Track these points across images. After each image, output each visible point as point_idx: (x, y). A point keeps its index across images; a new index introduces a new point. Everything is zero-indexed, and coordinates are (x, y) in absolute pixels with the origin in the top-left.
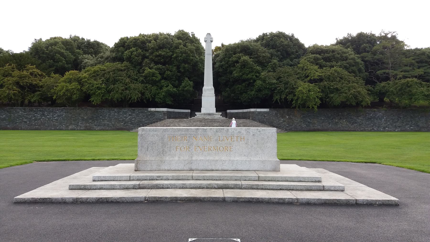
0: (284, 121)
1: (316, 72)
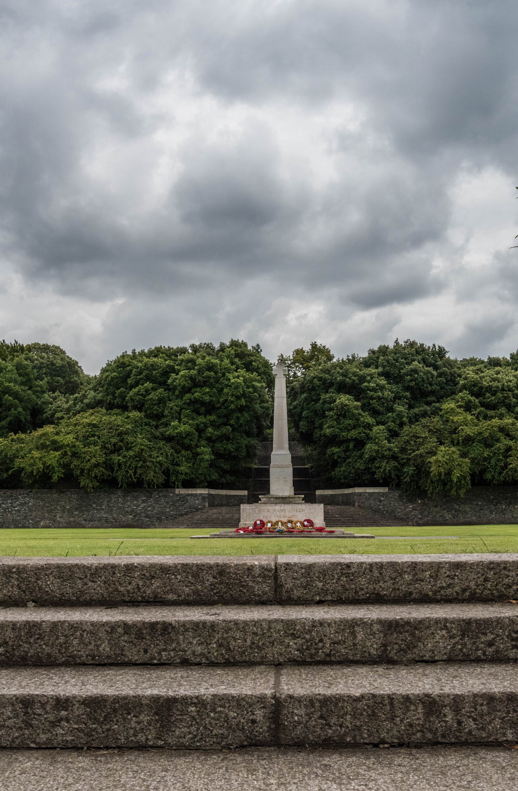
0: (414, 509)
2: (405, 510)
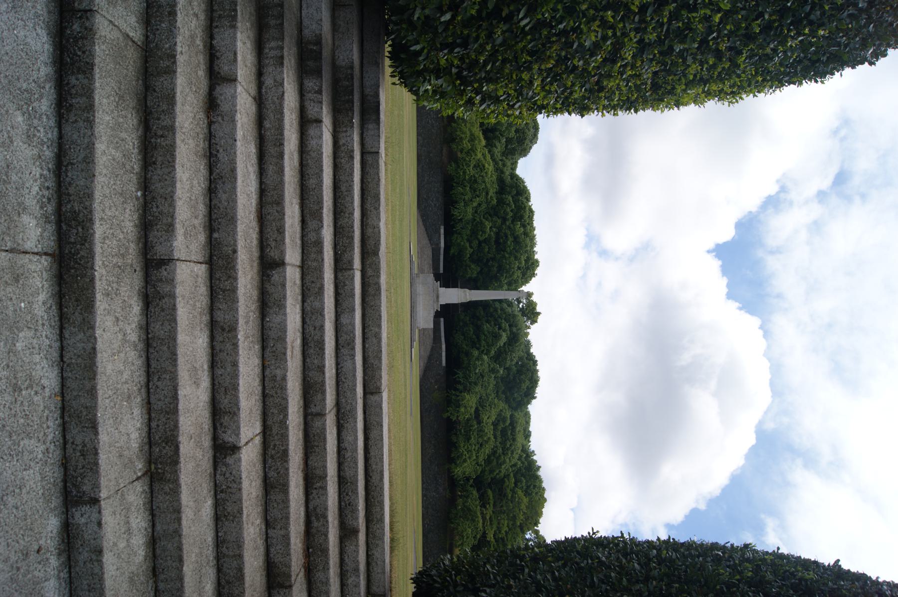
1: (489, 417)
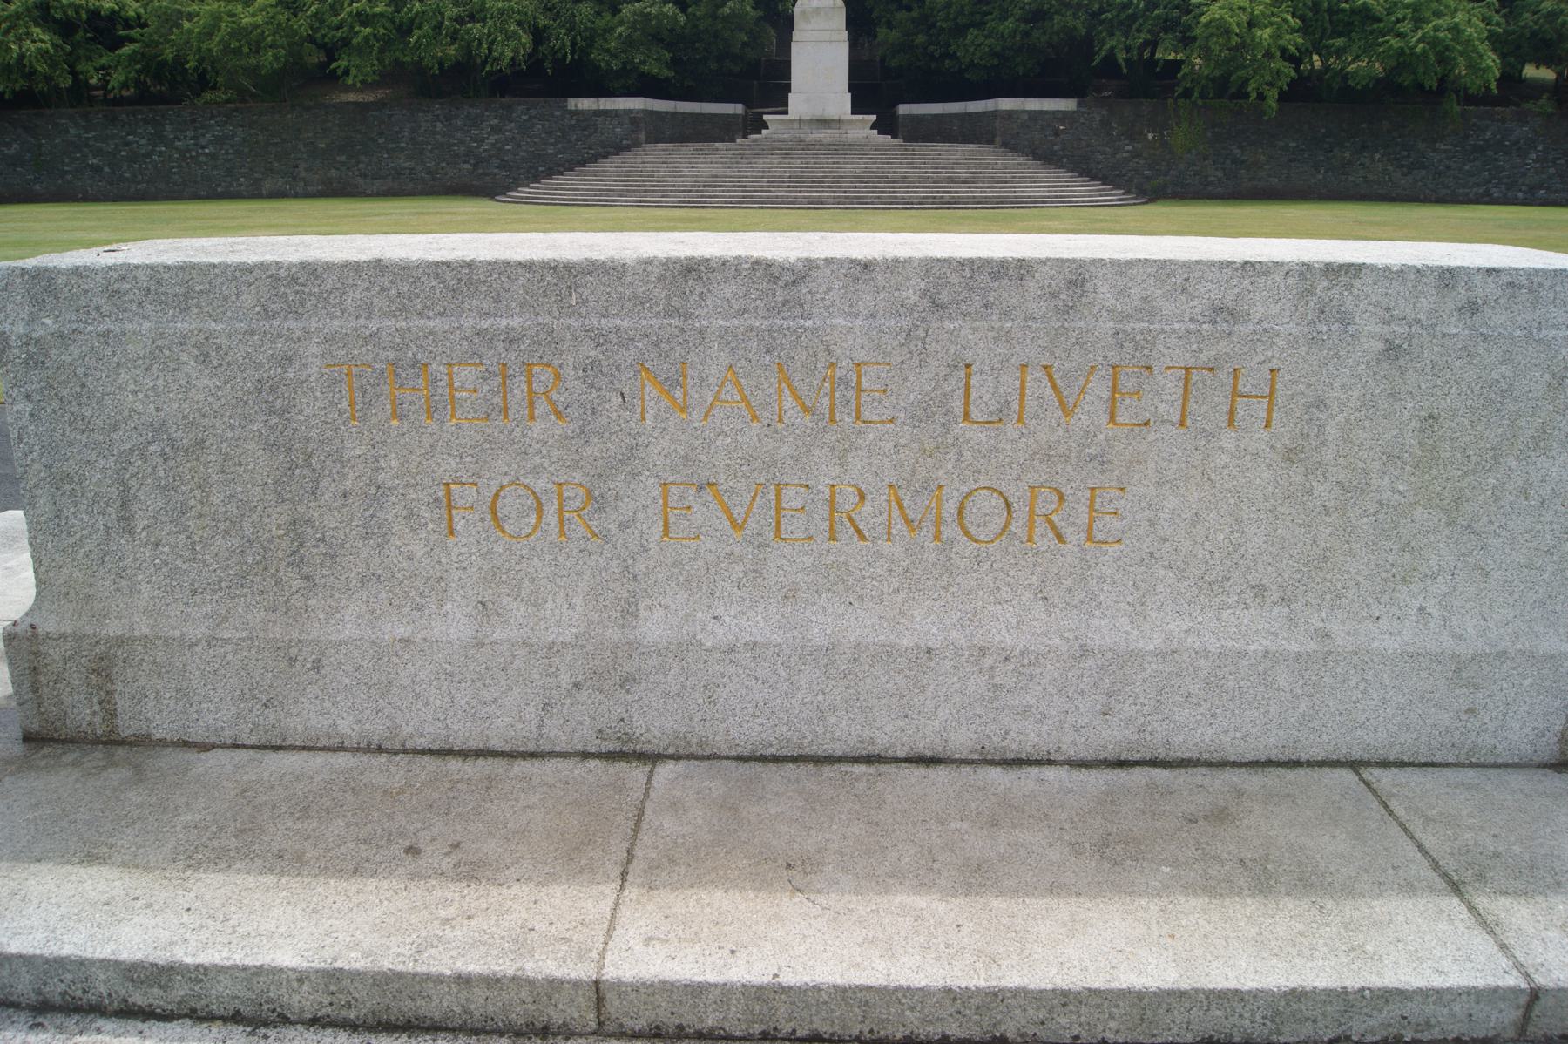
0: (1136, 155)
2: (1113, 155)
